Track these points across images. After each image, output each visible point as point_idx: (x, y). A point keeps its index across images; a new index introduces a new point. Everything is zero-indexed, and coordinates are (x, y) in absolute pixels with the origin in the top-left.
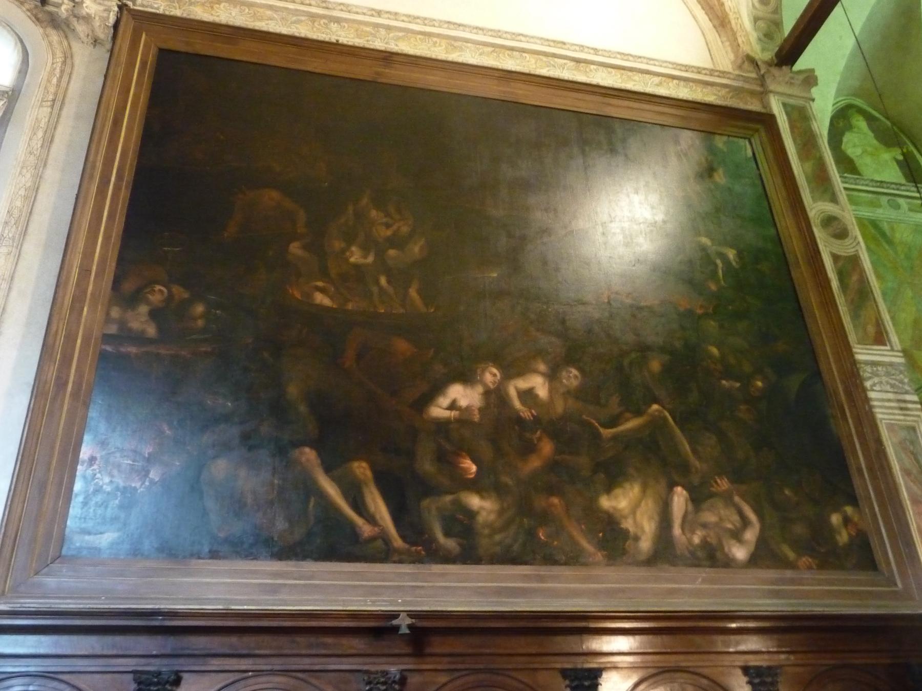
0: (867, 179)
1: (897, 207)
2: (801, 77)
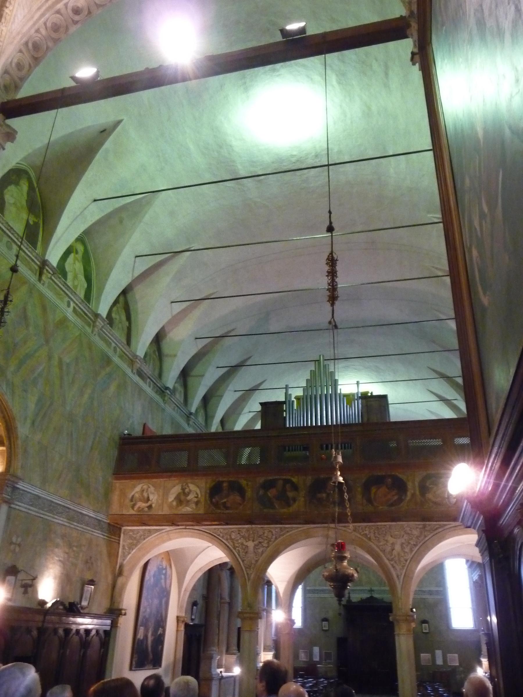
0: (5, 221)
1: (10, 248)
2: (8, 130)
